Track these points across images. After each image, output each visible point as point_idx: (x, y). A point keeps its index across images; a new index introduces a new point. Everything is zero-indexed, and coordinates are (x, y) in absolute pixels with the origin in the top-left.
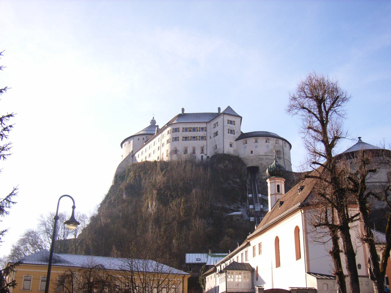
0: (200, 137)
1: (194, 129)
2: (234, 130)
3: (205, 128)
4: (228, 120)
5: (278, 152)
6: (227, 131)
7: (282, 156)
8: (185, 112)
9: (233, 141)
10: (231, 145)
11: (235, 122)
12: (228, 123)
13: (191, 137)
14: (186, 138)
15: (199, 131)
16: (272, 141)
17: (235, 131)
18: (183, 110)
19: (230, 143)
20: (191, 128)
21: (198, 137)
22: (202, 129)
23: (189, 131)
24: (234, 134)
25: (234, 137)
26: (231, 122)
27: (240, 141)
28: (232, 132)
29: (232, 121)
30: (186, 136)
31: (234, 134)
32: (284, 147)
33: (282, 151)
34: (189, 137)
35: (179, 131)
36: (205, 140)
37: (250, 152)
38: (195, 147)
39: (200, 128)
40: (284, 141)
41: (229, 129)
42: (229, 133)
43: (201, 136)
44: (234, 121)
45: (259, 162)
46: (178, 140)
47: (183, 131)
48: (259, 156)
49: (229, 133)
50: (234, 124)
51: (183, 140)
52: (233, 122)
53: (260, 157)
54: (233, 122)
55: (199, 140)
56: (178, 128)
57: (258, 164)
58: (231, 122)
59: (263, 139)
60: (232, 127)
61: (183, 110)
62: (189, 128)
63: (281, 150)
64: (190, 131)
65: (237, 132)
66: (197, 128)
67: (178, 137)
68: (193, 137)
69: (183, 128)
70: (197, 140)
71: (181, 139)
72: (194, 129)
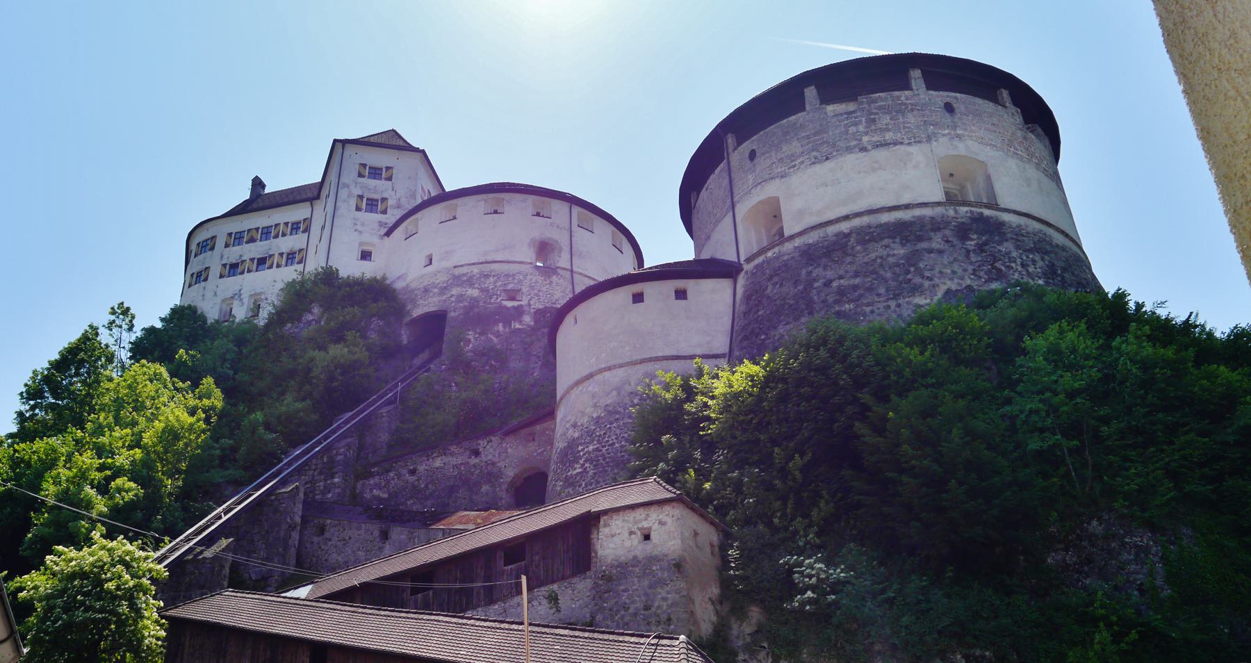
0: (281, 254)
1: (266, 233)
2: (384, 200)
3: (305, 220)
4: (364, 165)
5: (544, 248)
6: (353, 202)
7: (563, 261)
8: (267, 191)
9: (372, 239)
10: (366, 256)
11: (394, 171)
12: (360, 175)
13: (252, 260)
14: (233, 269)
15: (284, 235)
16: (517, 207)
17: (390, 202)
18: (258, 184)
19: (361, 244)
20: (257, 229)
21: (277, 256)
22: (295, 227)
23: (247, 242)
24: (384, 212)
25: (381, 224)
26: (375, 173)
27: (398, 233)
28: (372, 205)
29: (381, 169)
30: (234, 262)
31: (384, 212)
32: (575, 227)
33: (563, 240)
34: (243, 262)
35: (212, 249)
36: (300, 262)
37: (424, 261)
38: (261, 293)
39: (286, 224)
40: (576, 210)
41: (361, 197)
42: (358, 209)
43: (288, 251)
44: (388, 168)
45: (453, 293)
46: (206, 280)
47: (227, 246)
48: (455, 267)
49: (358, 209)
50: (389, 179)
51: (221, 276)
52: (384, 170)
53: (456, 274)
54: (384, 170)
55: (278, 266)
56: (214, 238)
57: (445, 301)
58: (375, 173)
59: (479, 201)
60: (377, 187)
61: (258, 184)
62: (249, 230)
63: (563, 240)
64: (252, 240)
65: (399, 207)
66: (277, 225)
67: (207, 269)
68: (258, 259)
69: (230, 235)
70: (271, 267)
71: (216, 270)
72: (266, 233)
